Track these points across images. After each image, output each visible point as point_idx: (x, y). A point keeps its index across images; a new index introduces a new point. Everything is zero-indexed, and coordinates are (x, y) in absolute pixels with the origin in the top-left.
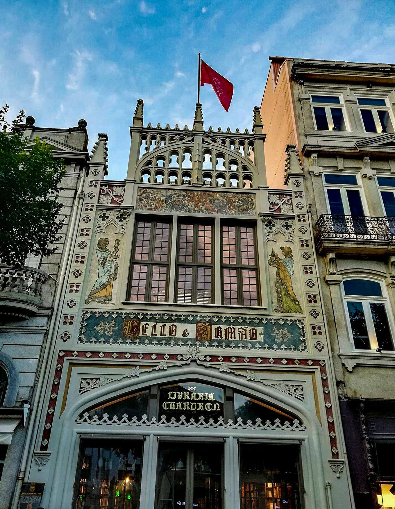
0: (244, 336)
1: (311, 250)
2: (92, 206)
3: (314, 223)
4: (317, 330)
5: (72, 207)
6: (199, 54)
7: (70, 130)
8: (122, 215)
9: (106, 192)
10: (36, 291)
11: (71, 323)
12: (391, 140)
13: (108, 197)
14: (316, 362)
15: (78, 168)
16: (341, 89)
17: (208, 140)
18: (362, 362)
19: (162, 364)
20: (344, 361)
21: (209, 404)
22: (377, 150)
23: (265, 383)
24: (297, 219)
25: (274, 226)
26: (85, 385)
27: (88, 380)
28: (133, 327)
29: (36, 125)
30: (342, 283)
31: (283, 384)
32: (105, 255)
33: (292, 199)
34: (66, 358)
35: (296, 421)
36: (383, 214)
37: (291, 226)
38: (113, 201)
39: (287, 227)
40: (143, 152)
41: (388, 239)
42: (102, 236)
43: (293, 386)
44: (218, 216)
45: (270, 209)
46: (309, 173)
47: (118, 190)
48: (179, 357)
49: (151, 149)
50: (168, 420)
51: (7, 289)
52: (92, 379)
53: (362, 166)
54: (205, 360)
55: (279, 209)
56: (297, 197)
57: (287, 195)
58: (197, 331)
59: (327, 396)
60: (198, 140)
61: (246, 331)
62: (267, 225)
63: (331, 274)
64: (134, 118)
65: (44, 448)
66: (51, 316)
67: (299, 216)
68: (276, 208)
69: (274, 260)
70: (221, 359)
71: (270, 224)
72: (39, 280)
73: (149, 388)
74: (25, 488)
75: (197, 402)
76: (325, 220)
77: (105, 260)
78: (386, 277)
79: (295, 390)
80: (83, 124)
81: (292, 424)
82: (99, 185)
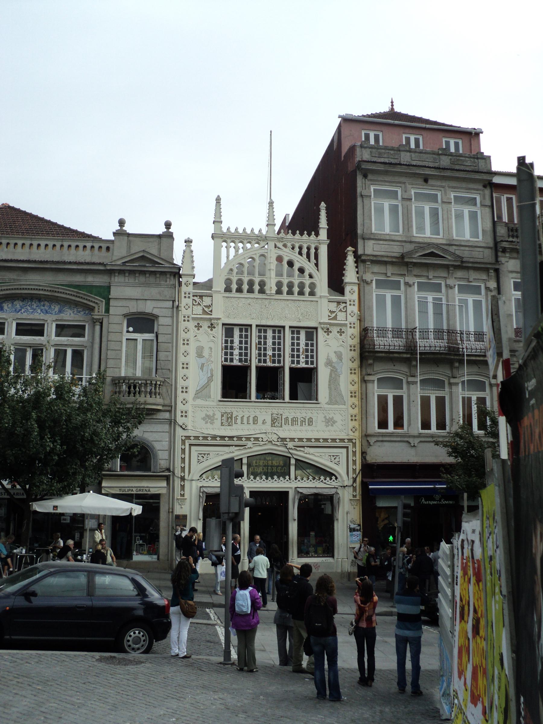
0: (304, 423)
1: (356, 354)
2: (188, 317)
3: (362, 329)
4: (353, 418)
5: (172, 317)
6: (271, 132)
7: (159, 236)
8: (212, 324)
9: (197, 303)
10: (159, 395)
11: (186, 416)
12: (432, 250)
13: (199, 307)
14: (350, 440)
15: (172, 278)
16: (400, 183)
17: (280, 245)
18: (381, 439)
19: (250, 444)
20: (369, 439)
21: (280, 468)
22: (419, 261)
23: (317, 454)
24: (349, 325)
25: (331, 332)
26: (200, 458)
27: (203, 455)
28: (228, 418)
29: (129, 228)
30: (376, 382)
31: (327, 456)
32: (203, 360)
33: (346, 306)
34: (186, 441)
35: (334, 478)
36: (414, 321)
37: (343, 332)
38: (205, 312)
39: (341, 332)
40: (224, 260)
41: (412, 350)
42: (198, 344)
43: (333, 456)
44: (287, 324)
45: (329, 316)
46: (363, 280)
47: (207, 301)
48: (261, 440)
49: (231, 257)
50: (255, 478)
51: (143, 395)
52: (205, 454)
53: (406, 273)
54: (278, 441)
55: (335, 318)
56: (350, 305)
57: (343, 303)
58: (272, 421)
59: (354, 462)
60: (272, 244)
61: (305, 419)
62: (325, 332)
63: (369, 375)
64: (214, 222)
65: (183, 495)
66: (171, 411)
67: (350, 324)
68: (334, 315)
69: (329, 363)
70: (288, 440)
71: (328, 331)
72: (160, 385)
73: (241, 459)
74: (178, 517)
75: (271, 466)
76: (369, 331)
77: (203, 365)
78: (407, 375)
79: (335, 459)
80: (168, 225)
81: (331, 479)
82: (191, 295)
